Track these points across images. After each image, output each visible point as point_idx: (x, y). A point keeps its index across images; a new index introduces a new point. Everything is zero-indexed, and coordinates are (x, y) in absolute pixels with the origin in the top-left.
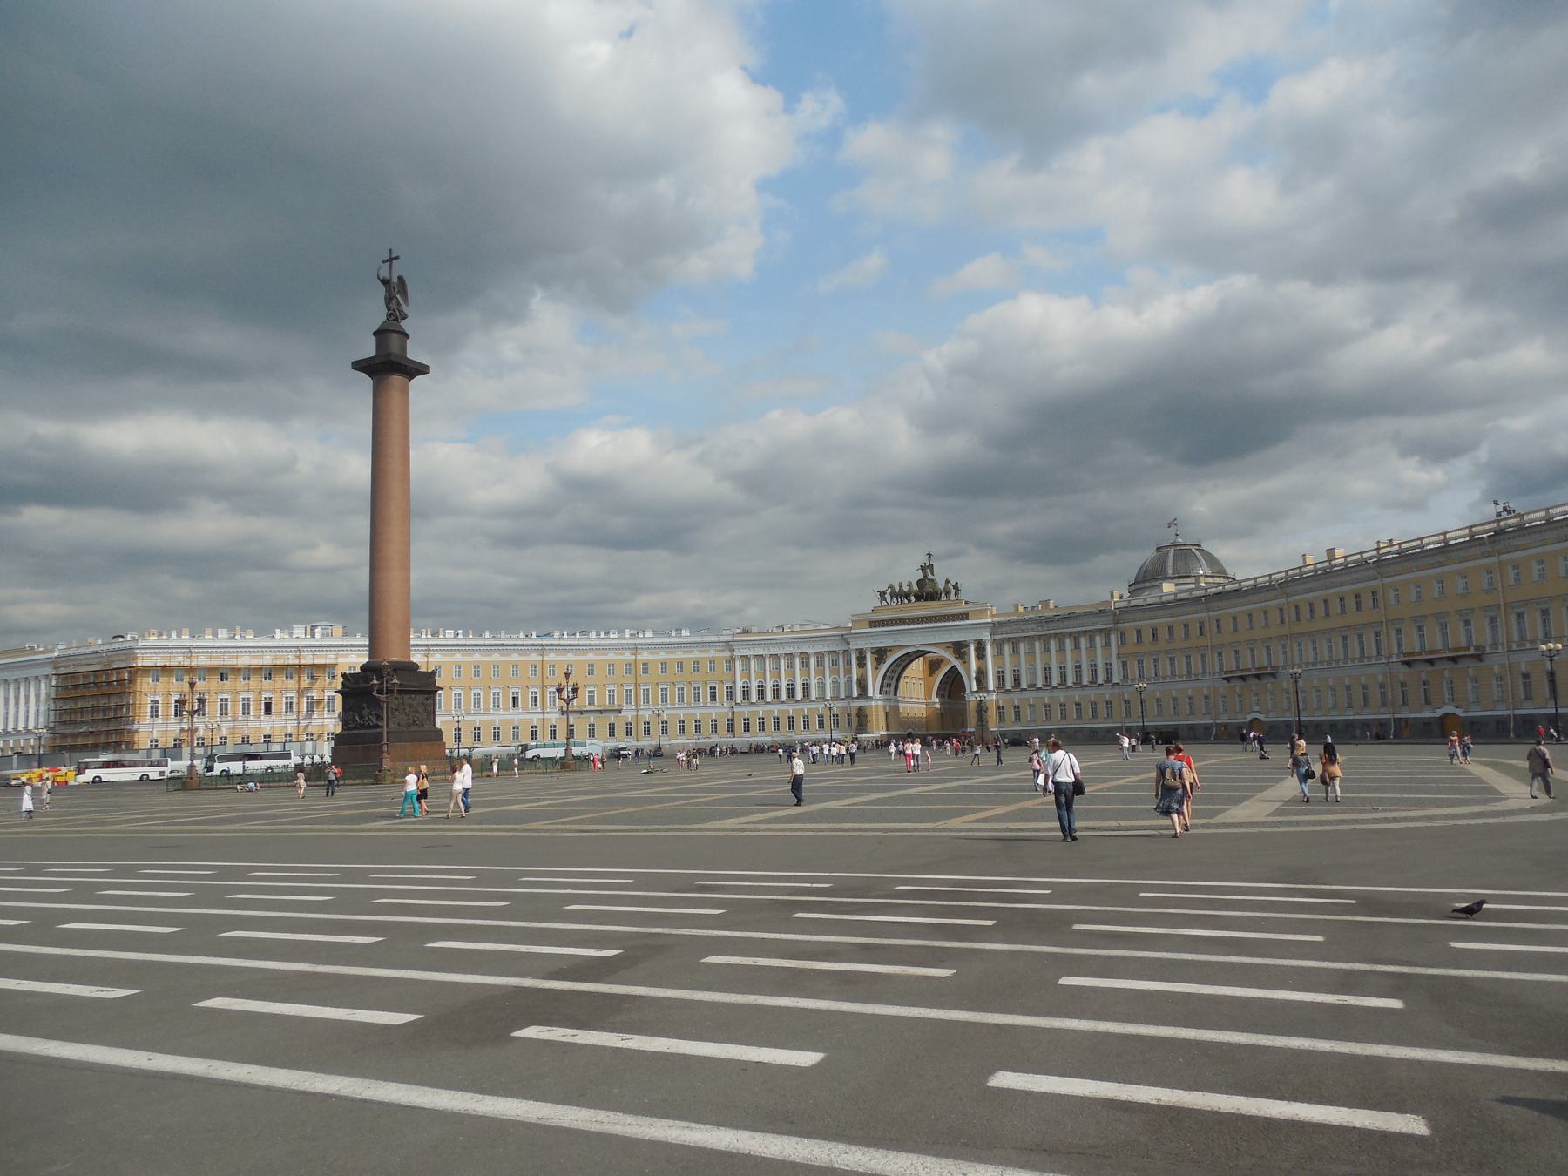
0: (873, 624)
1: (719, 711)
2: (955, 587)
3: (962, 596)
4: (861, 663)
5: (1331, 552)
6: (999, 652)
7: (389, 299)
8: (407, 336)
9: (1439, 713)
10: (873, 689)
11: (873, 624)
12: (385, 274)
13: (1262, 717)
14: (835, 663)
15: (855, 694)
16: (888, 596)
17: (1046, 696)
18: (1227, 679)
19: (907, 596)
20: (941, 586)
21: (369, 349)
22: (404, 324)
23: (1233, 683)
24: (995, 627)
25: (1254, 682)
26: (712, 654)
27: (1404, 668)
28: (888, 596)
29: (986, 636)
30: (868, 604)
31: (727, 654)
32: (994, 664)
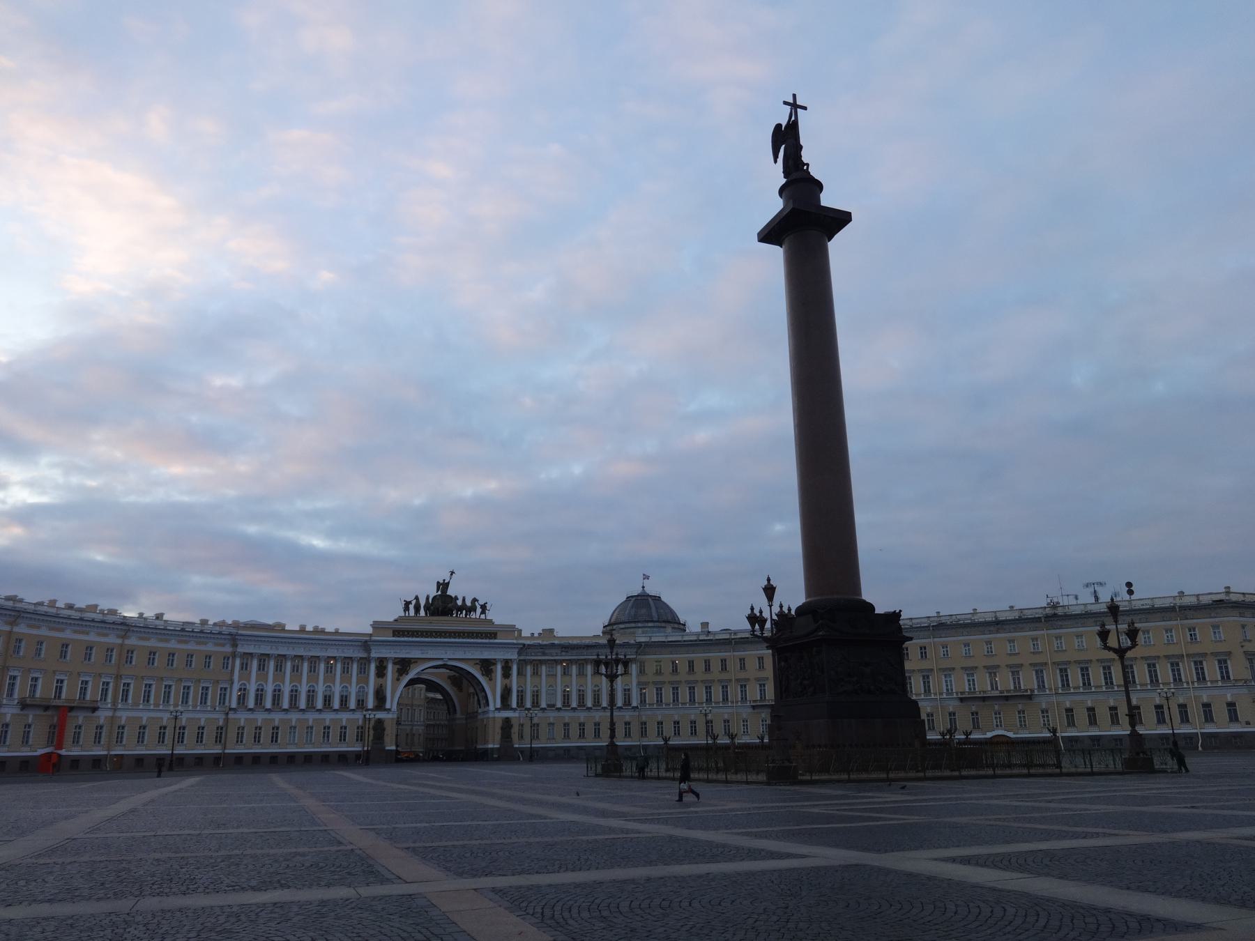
0: (397, 633)
1: (209, 717)
2: (484, 607)
3: (490, 615)
4: (381, 672)
6: (521, 673)
9: (989, 735)
11: (397, 633)
14: (346, 670)
17: (567, 715)
18: (754, 707)
20: (468, 603)
24: (523, 649)
26: (210, 647)
27: (957, 703)
28: (411, 607)
30: (393, 612)
31: (228, 649)
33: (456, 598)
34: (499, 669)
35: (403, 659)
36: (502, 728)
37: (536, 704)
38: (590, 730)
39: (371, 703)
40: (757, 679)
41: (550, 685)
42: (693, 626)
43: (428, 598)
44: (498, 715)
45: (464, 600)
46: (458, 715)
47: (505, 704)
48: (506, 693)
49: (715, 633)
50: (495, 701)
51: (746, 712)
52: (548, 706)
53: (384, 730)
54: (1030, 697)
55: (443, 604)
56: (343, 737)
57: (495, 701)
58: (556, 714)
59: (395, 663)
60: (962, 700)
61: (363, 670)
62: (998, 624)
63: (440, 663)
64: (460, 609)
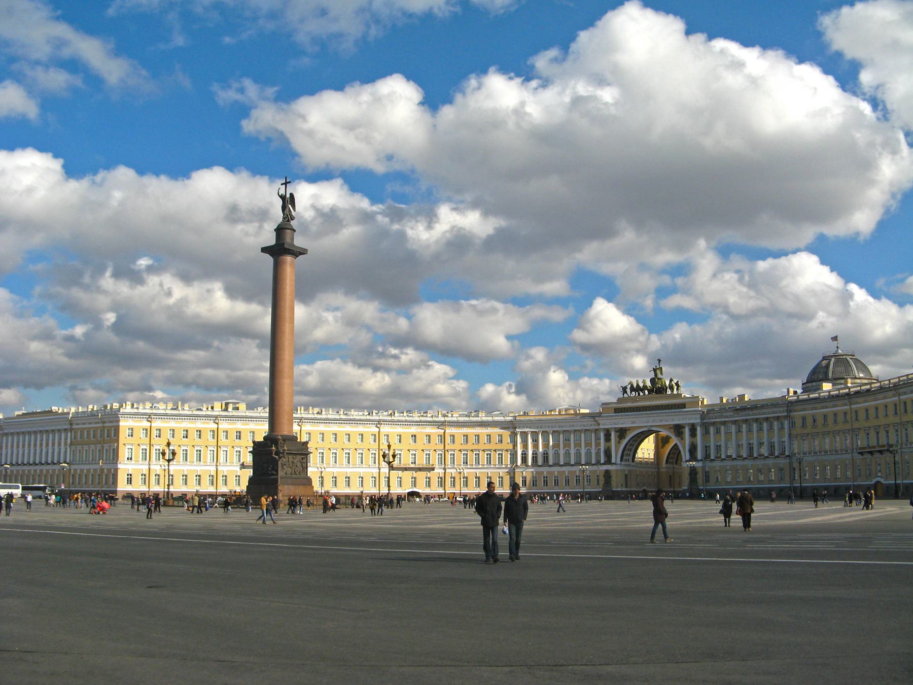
0: (617, 410)
2: (677, 384)
3: (682, 390)
6: (706, 432)
7: (284, 208)
8: (295, 231)
11: (617, 410)
12: (282, 192)
13: (882, 481)
15: (602, 461)
16: (628, 390)
19: (642, 390)
20: (667, 383)
21: (270, 239)
22: (292, 222)
25: (877, 455)
28: (628, 390)
29: (696, 420)
35: (621, 429)
36: (690, 474)
47: (693, 457)
48: (693, 449)
50: (685, 455)
52: (728, 457)
53: (610, 477)
57: (685, 455)
61: (597, 439)
63: (646, 429)
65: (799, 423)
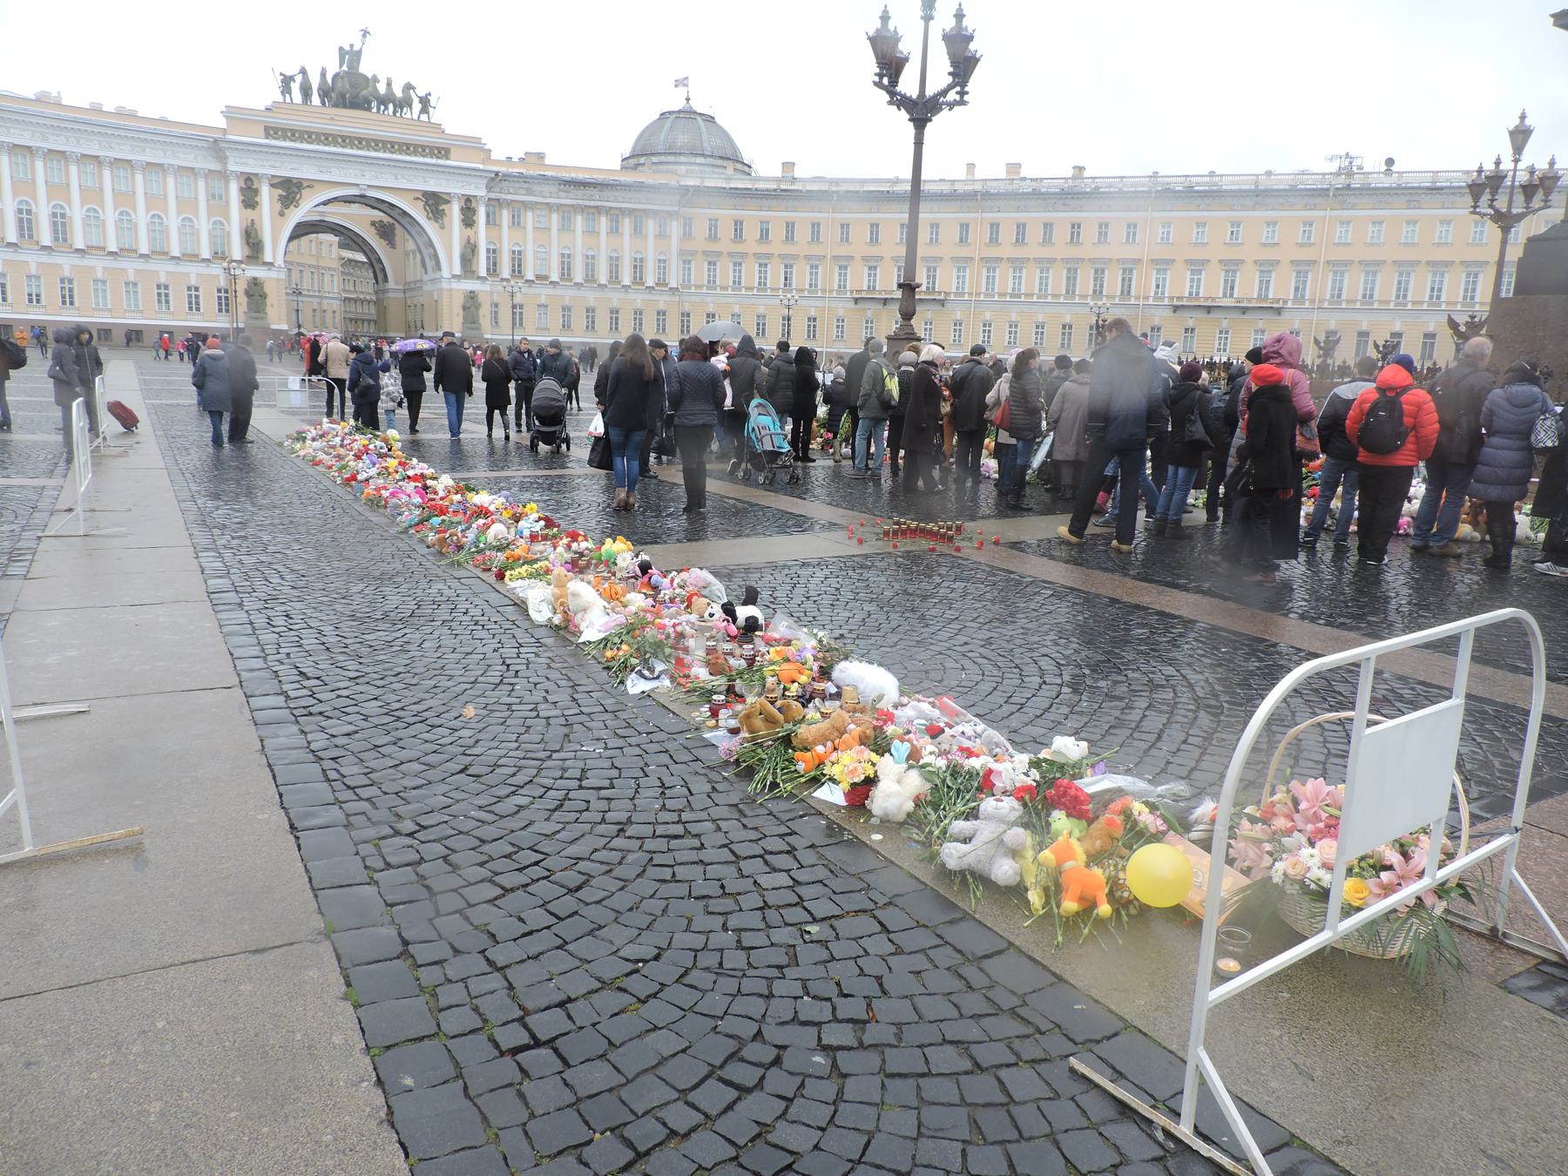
0: (270, 131)
2: (425, 102)
3: (436, 116)
4: (250, 199)
5: (1014, 168)
6: (491, 221)
10: (274, 250)
11: (271, 131)
16: (295, 87)
17: (567, 294)
18: (856, 300)
23: (861, 305)
24: (495, 179)
27: (1168, 313)
28: (295, 87)
29: (478, 190)
30: (262, 94)
32: (487, 237)
33: (376, 79)
34: (455, 211)
36: (464, 308)
37: (517, 271)
38: (603, 321)
39: (237, 250)
40: (865, 259)
41: (539, 242)
42: (766, 167)
43: (323, 75)
44: (455, 285)
45: (389, 84)
46: (391, 284)
48: (469, 251)
49: (801, 180)
50: (451, 264)
51: (843, 307)
52: (538, 277)
53: (264, 296)
54: (1278, 311)
55: (350, 91)
56: (194, 305)
57: (451, 264)
58: (550, 291)
59: (272, 185)
60: (1176, 309)
62: (1260, 195)
64: (383, 101)
65: (701, 230)
